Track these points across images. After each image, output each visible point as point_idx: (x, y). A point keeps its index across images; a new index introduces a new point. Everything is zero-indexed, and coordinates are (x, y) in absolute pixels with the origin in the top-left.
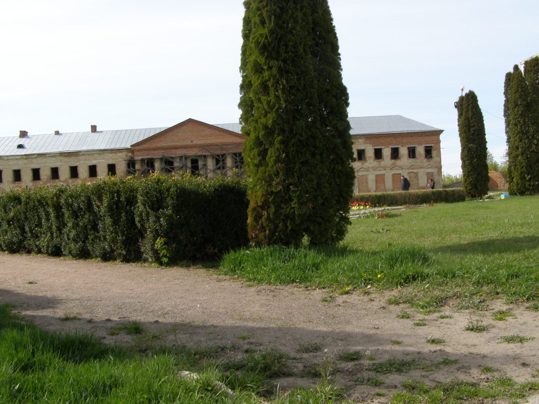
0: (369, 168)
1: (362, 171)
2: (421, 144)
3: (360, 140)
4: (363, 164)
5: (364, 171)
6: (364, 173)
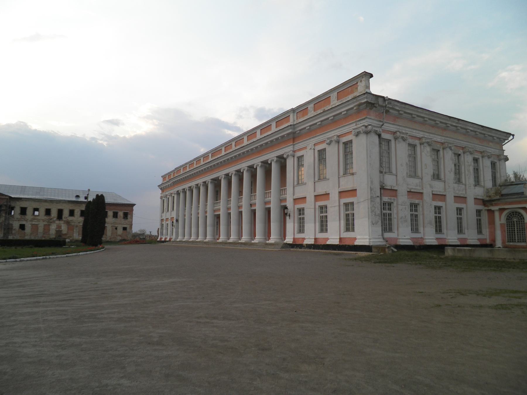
2: (121, 210)
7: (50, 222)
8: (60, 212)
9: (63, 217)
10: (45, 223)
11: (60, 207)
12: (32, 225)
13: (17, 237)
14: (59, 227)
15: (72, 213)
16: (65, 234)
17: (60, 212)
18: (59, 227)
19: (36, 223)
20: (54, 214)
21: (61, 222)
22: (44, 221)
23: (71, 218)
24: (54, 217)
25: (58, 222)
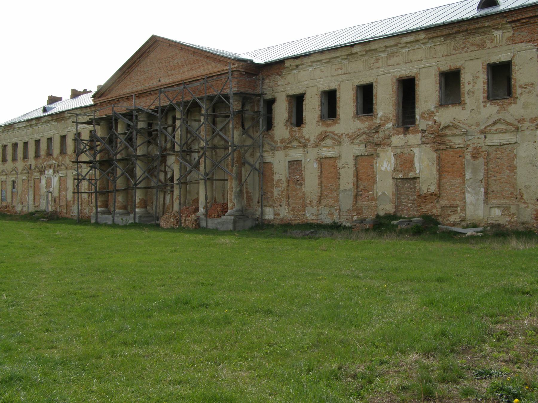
0: (523, 120)
1: (496, 132)
3: (497, 34)
4: (503, 108)
5: (505, 132)
6: (506, 138)
7: (375, 143)
8: (407, 88)
9: (418, 112)
10: (359, 149)
11: (405, 71)
12: (321, 161)
13: (285, 213)
14: (405, 162)
15: (451, 80)
16: (436, 196)
17: (407, 88)
18: (405, 162)
19: (332, 153)
20: (386, 102)
21: (414, 138)
22: (352, 138)
23: (448, 115)
24: (387, 120)
25: (397, 140)
